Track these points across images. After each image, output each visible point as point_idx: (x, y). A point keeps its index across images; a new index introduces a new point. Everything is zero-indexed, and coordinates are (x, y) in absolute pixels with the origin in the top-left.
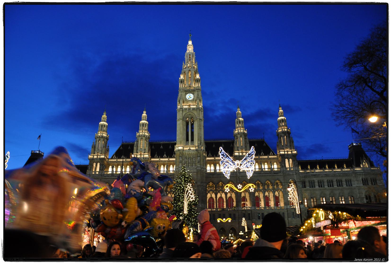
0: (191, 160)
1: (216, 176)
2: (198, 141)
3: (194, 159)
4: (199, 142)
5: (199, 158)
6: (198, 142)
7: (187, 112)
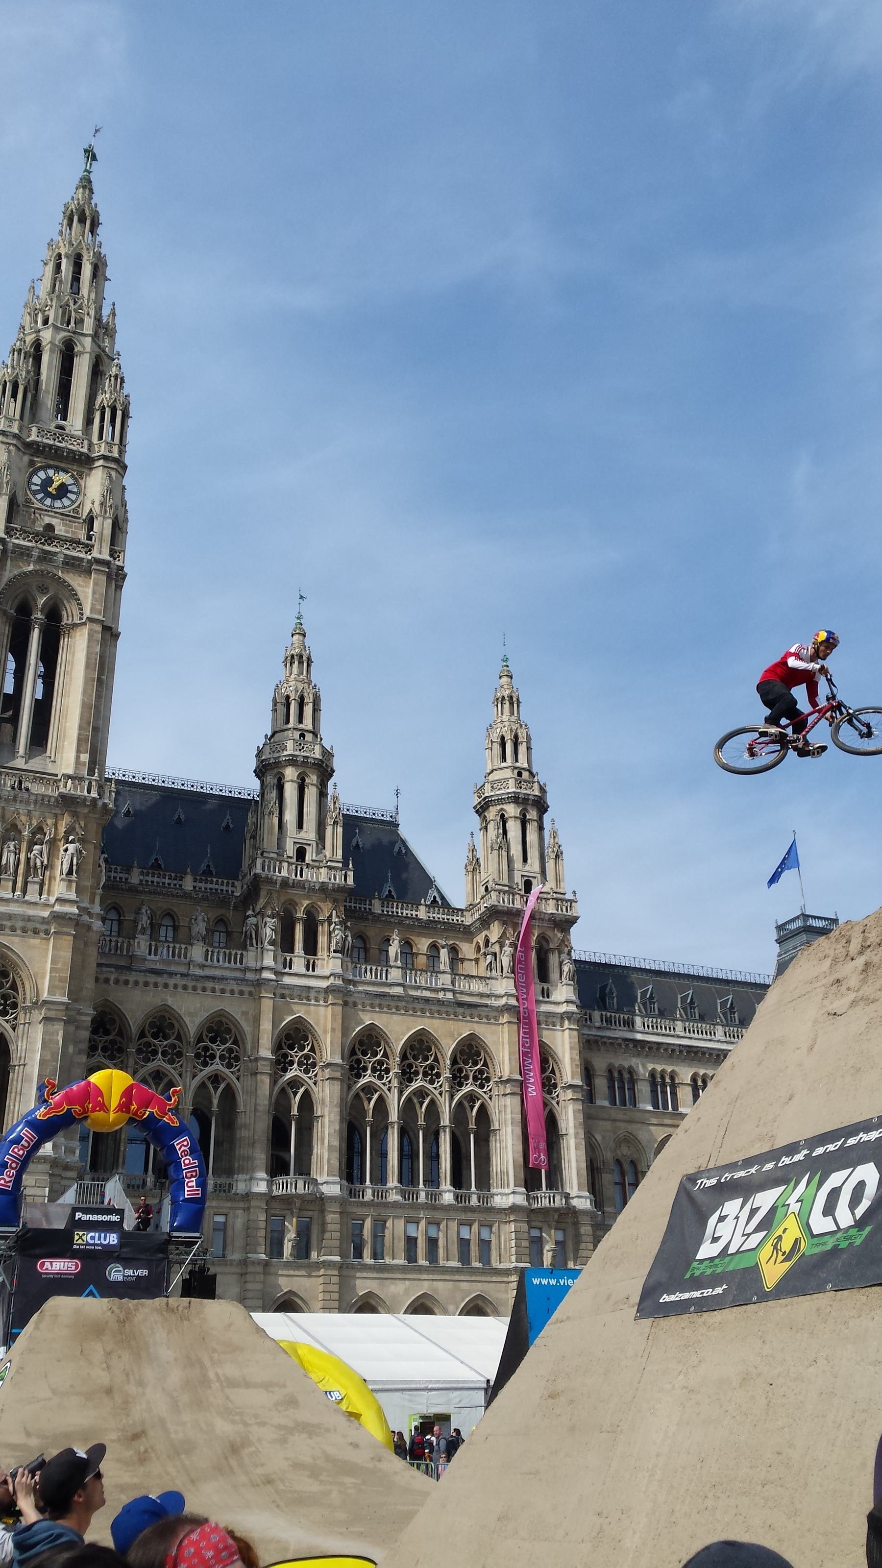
0: (17, 852)
1: (141, 979)
2: (78, 751)
3: (36, 847)
4: (85, 757)
5: (71, 847)
6: (78, 758)
7: (31, 568)
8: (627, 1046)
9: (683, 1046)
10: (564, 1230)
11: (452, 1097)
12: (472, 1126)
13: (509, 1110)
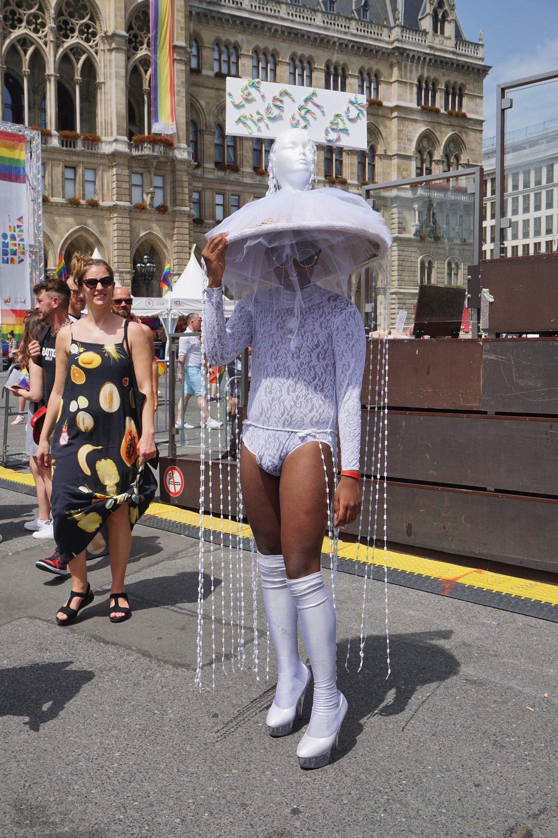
8: (234, 22)
9: (285, 27)
10: (163, 176)
11: (57, 47)
12: (78, 77)
13: (113, 65)
